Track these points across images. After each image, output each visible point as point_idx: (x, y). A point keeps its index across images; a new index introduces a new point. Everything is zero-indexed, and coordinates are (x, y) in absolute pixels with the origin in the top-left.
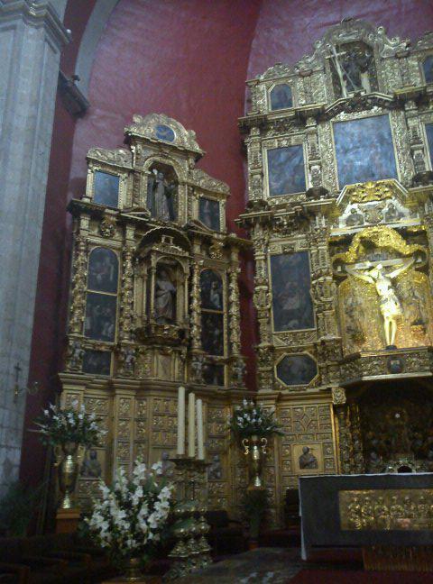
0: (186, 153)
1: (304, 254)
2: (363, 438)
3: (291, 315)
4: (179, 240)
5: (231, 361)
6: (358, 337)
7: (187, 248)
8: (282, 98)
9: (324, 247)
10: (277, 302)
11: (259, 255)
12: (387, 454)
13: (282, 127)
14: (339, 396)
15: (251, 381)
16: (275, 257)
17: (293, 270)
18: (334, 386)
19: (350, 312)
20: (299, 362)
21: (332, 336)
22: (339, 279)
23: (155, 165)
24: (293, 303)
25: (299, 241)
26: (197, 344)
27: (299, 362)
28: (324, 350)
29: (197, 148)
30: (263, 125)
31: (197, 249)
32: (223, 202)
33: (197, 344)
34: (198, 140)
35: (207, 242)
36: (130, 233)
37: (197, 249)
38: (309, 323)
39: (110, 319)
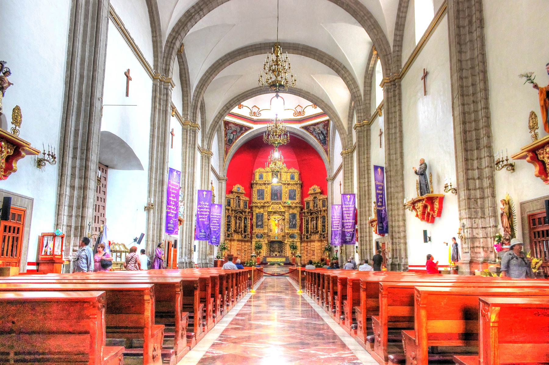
0: (242, 193)
1: (263, 214)
2: (270, 249)
3: (259, 225)
4: (241, 213)
5: (248, 234)
6: (271, 231)
7: (242, 214)
8: (261, 177)
9: (266, 214)
10: (257, 223)
11: (254, 213)
12: (273, 252)
13: (261, 185)
14: (266, 242)
15: (251, 238)
16: (257, 214)
17: (260, 217)
18: (266, 240)
19: (270, 226)
20: (260, 235)
21: (266, 231)
22: (268, 219)
23: (237, 196)
24: (259, 223)
25: (262, 210)
26: (243, 232)
27: (260, 235)
28: (265, 234)
29: (244, 192)
30: (256, 184)
31: (244, 214)
32: (248, 202)
33: (243, 232)
34: (245, 190)
35: (245, 212)
36: (233, 212)
37: (244, 214)
38: (262, 227)
39: (230, 228)
